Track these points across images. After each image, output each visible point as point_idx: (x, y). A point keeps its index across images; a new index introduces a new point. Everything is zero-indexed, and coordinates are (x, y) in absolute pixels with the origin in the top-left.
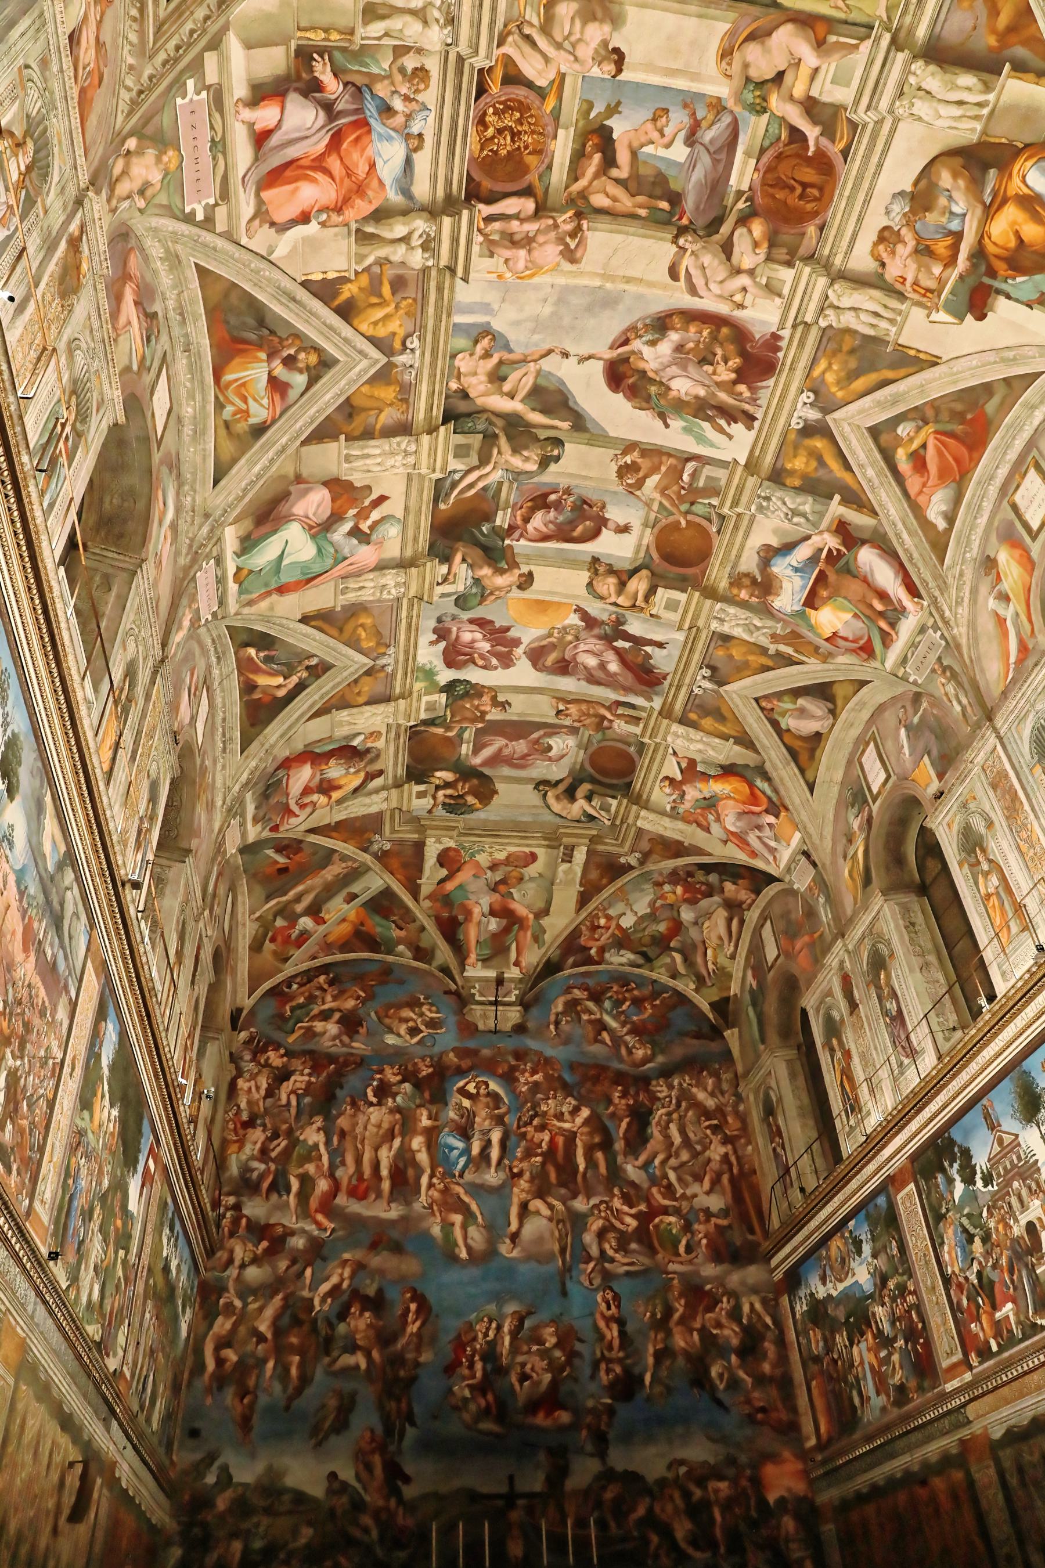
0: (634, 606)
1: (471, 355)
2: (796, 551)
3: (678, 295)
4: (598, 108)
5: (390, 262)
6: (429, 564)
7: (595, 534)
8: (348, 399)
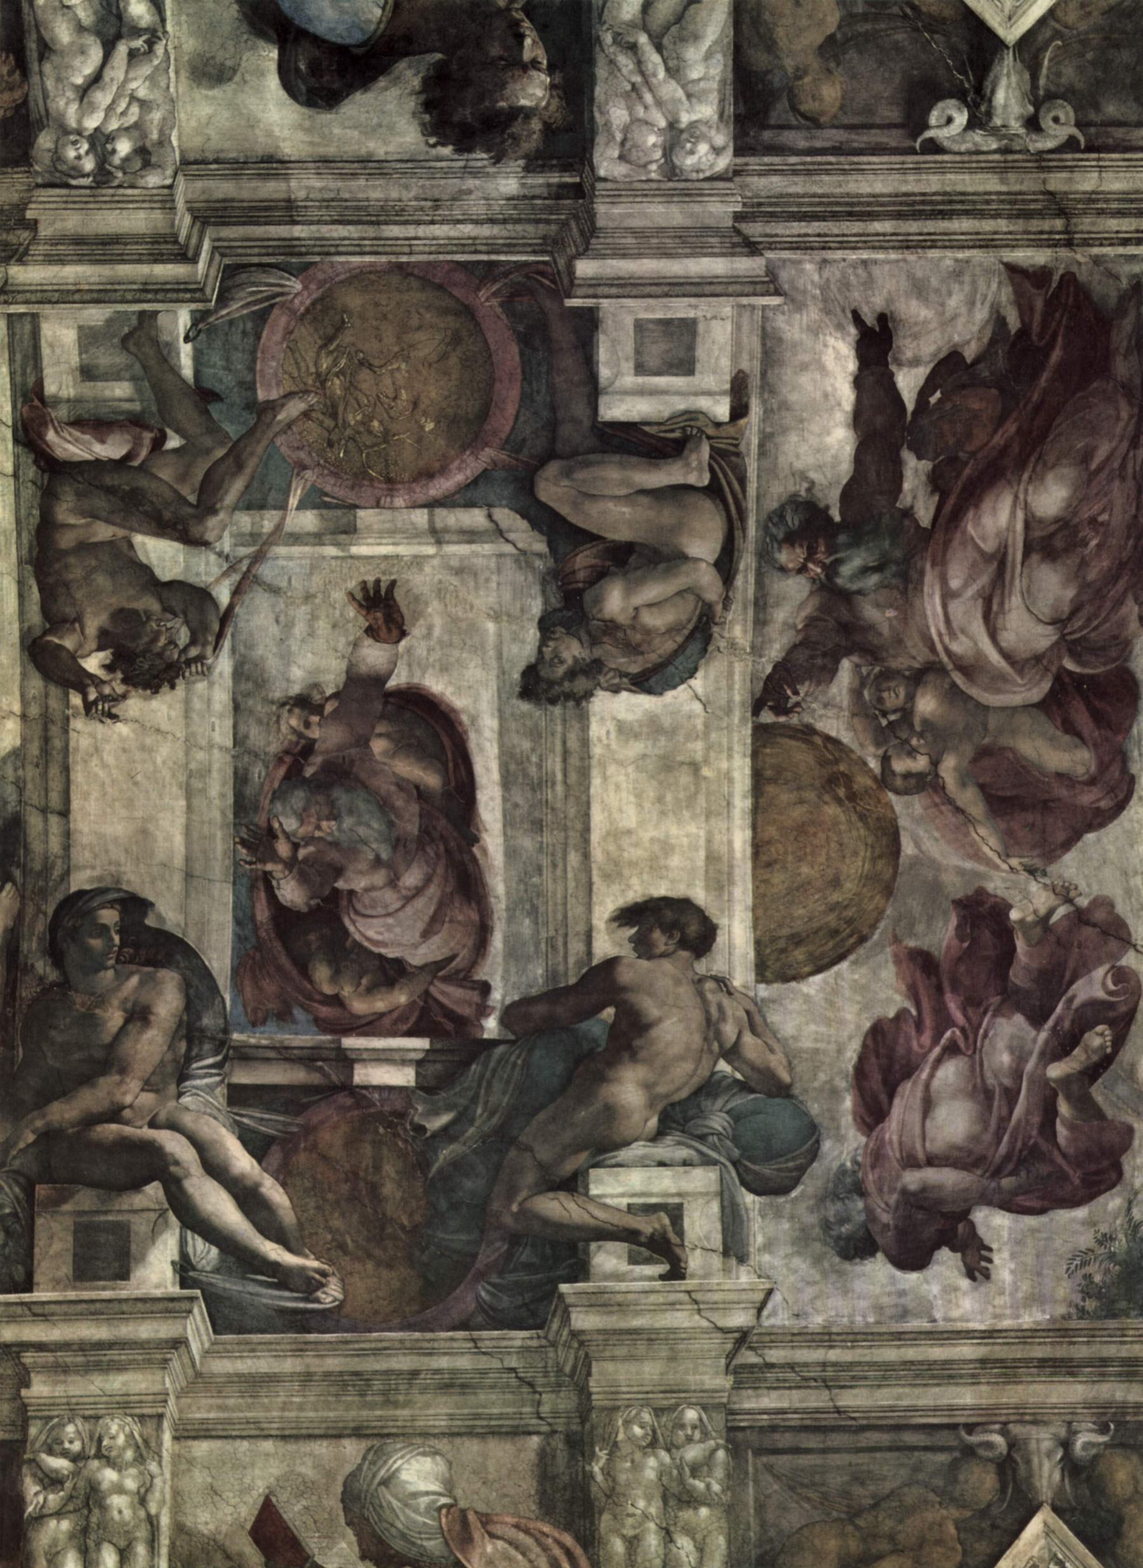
0: (714, 490)
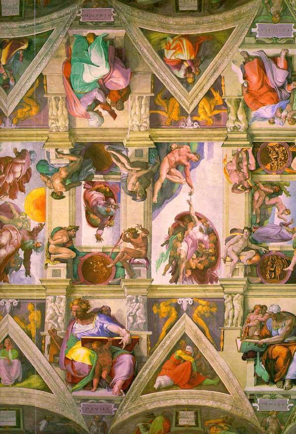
1: (189, 152)
4: (288, 188)
6: (70, 143)
7: (93, 226)
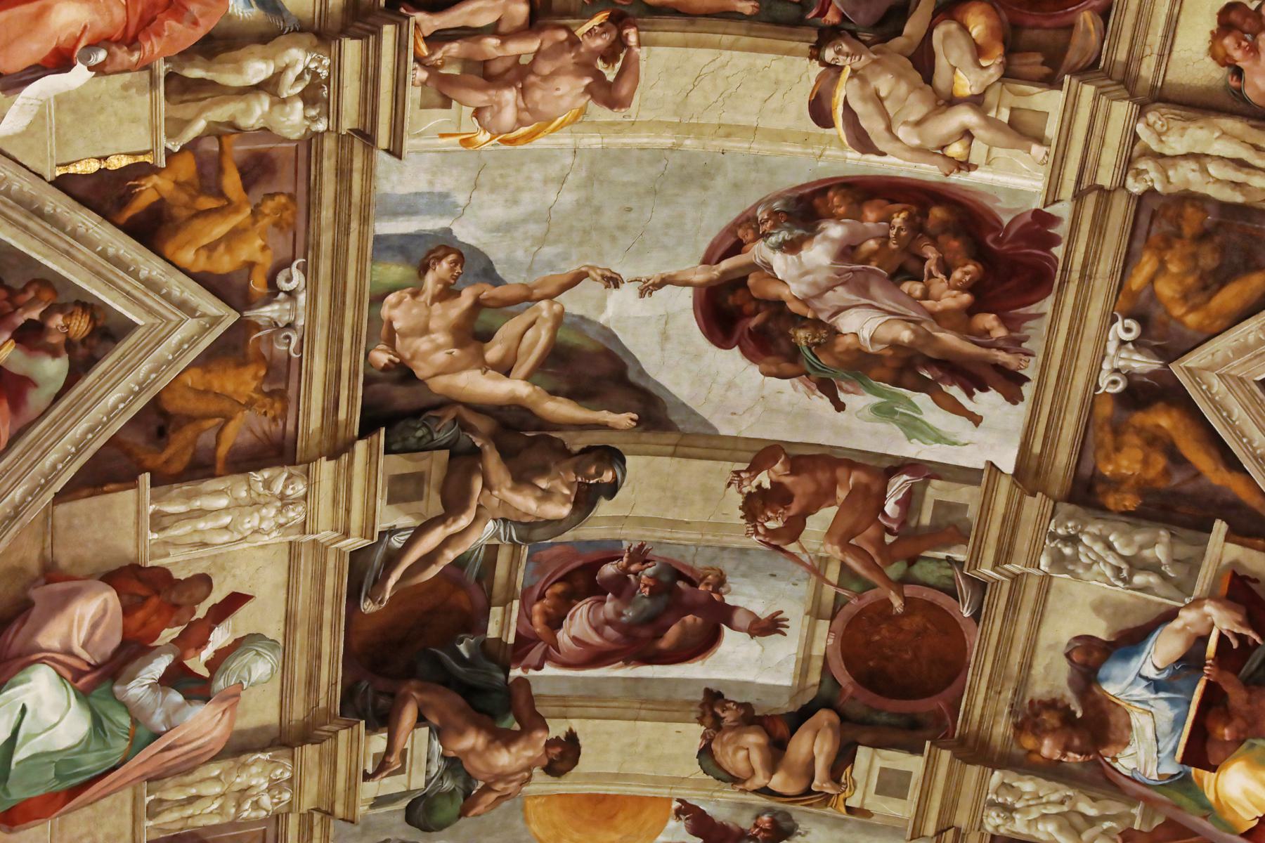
0: (808, 791)
1: (415, 294)
2: (1149, 645)
3: (832, 151)
5: (239, 130)
6: (343, 735)
8: (156, 400)
